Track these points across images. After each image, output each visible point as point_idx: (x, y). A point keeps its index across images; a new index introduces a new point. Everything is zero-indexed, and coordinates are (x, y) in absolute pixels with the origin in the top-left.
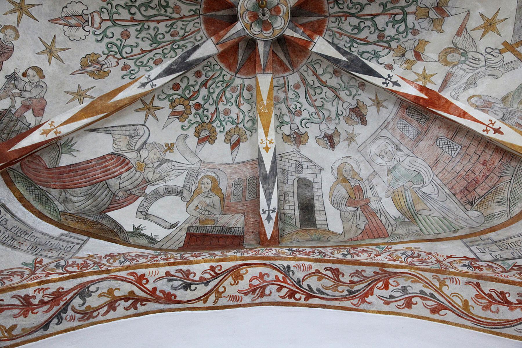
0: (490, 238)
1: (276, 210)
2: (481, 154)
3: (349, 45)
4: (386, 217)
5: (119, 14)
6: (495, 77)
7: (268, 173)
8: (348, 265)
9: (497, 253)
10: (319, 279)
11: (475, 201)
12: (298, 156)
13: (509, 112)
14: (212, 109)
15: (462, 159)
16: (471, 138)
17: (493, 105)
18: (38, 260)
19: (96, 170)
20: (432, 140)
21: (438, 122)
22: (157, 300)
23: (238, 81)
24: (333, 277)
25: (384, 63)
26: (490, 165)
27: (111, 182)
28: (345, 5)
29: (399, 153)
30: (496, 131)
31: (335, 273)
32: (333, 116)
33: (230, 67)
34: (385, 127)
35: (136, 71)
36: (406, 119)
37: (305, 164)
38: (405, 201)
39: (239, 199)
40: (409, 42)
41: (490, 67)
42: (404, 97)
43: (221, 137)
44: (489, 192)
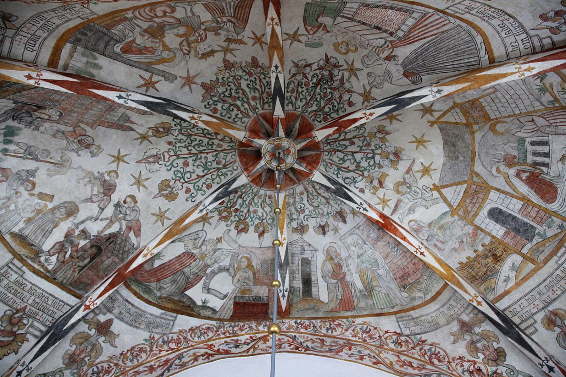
3: (336, 173)
4: (355, 289)
5: (181, 151)
6: (426, 207)
9: (414, 328)
10: (313, 343)
13: (431, 235)
14: (245, 210)
18: (152, 336)
19: (175, 265)
22: (221, 353)
23: (262, 192)
27: (185, 270)
28: (335, 145)
29: (365, 246)
30: (422, 254)
32: (325, 213)
33: (257, 184)
35: (195, 194)
36: (371, 227)
37: (306, 247)
40: (376, 173)
41: (424, 199)
43: (252, 229)
44: (415, 282)
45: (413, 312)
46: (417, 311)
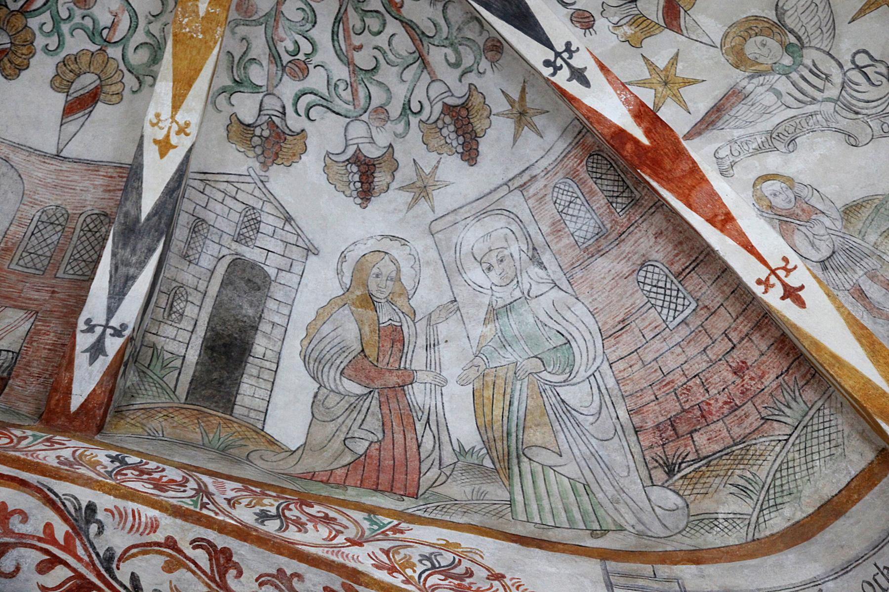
0: (677, 579)
1: (127, 333)
2: (740, 342)
4: (438, 440)
6: (852, 140)
7: (143, 216)
8: (261, 550)
10: (169, 568)
11: (683, 465)
12: (257, 193)
15: (689, 340)
16: (728, 290)
17: (814, 217)
20: (630, 264)
21: (658, 218)
24: (208, 571)
25: (574, 3)
26: (752, 379)
29: (535, 271)
30: (791, 293)
31: (217, 560)
32: (395, 110)
34: (521, 186)
36: (581, 183)
37: (269, 221)
38: (507, 408)
39: (39, 266)
41: (849, 108)
42: (588, 118)
45: (692, 569)
46: (709, 569)
